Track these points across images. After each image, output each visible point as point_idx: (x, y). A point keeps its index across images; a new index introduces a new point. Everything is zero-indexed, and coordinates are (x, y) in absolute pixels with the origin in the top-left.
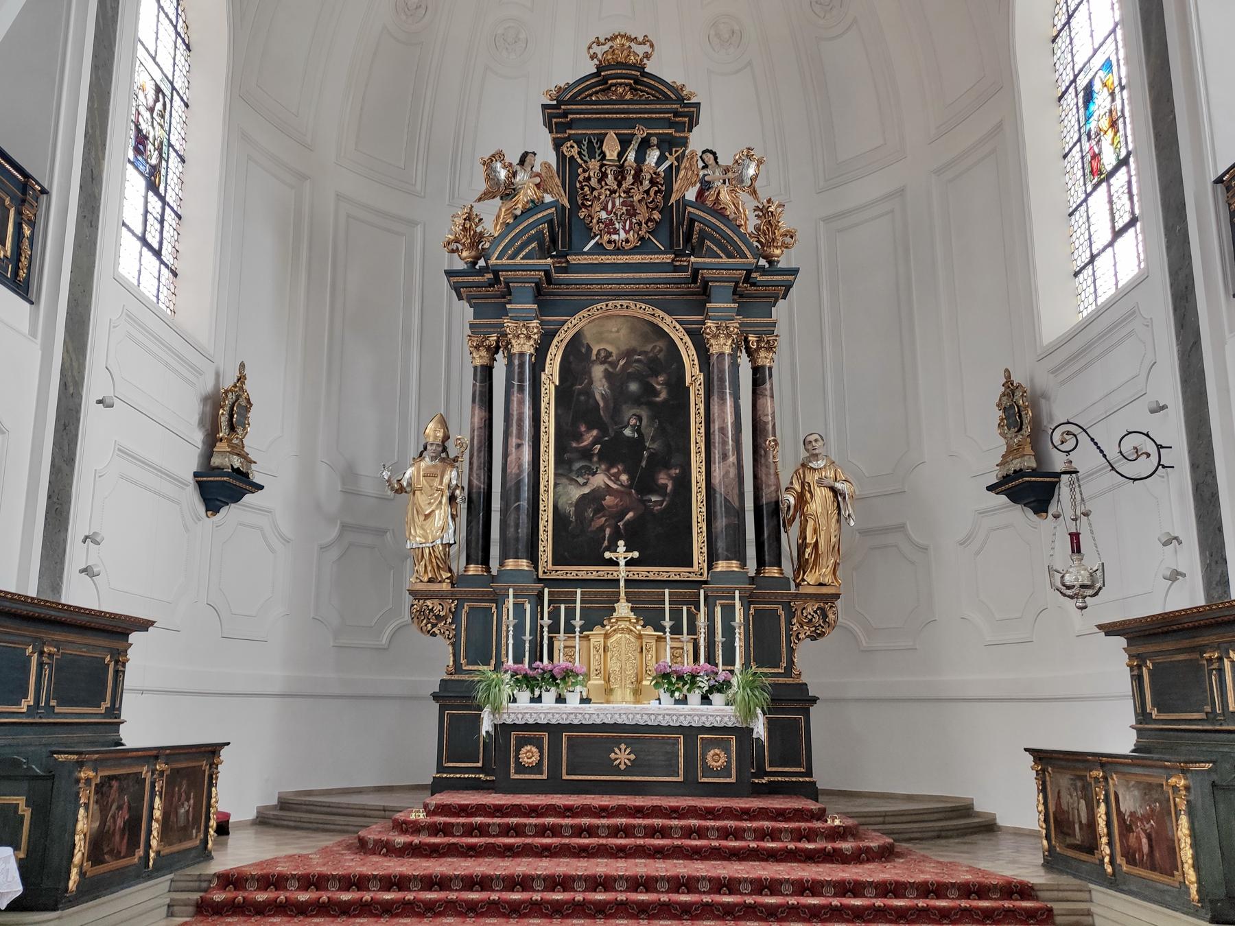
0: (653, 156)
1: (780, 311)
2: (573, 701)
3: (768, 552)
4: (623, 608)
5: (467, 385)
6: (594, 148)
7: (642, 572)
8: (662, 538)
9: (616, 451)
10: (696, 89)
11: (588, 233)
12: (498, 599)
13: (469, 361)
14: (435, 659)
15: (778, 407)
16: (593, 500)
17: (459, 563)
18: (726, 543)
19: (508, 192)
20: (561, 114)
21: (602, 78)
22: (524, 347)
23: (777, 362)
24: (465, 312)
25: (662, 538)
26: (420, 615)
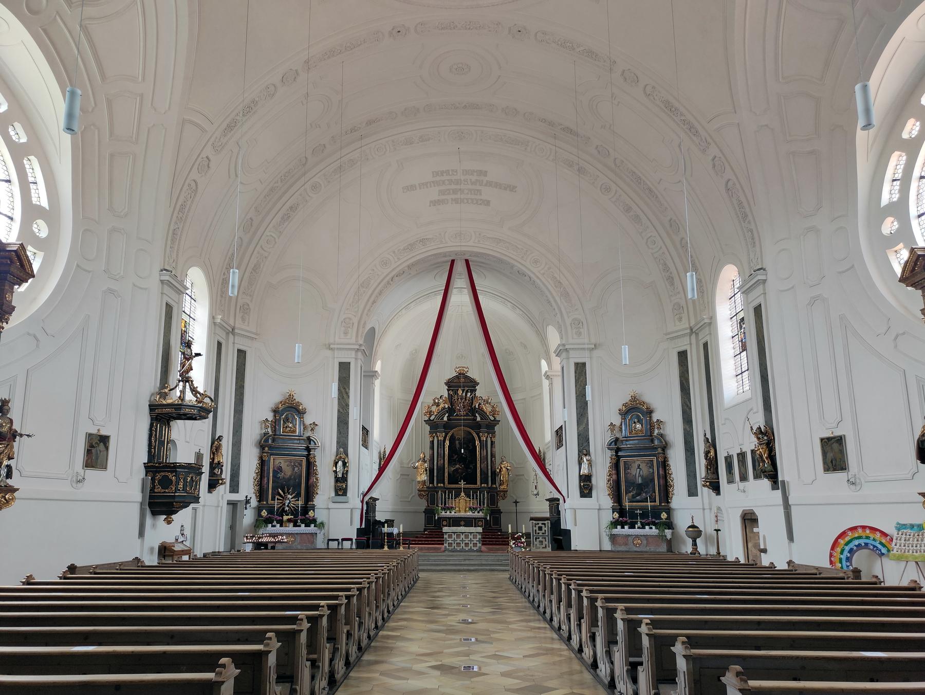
0: (469, 394)
1: (496, 428)
2: (453, 513)
3: (494, 482)
4: (463, 494)
5: (428, 445)
6: (456, 392)
7: (468, 486)
8: (471, 479)
9: (461, 459)
10: (478, 380)
11: (455, 412)
12: (437, 493)
13: (428, 439)
14: (423, 504)
15: (497, 450)
16: (457, 469)
17: (428, 484)
18: (484, 480)
19: (438, 405)
20: (450, 384)
21: (457, 377)
22: (441, 438)
23: (497, 440)
24: (428, 428)
25: (471, 479)
26: (420, 495)
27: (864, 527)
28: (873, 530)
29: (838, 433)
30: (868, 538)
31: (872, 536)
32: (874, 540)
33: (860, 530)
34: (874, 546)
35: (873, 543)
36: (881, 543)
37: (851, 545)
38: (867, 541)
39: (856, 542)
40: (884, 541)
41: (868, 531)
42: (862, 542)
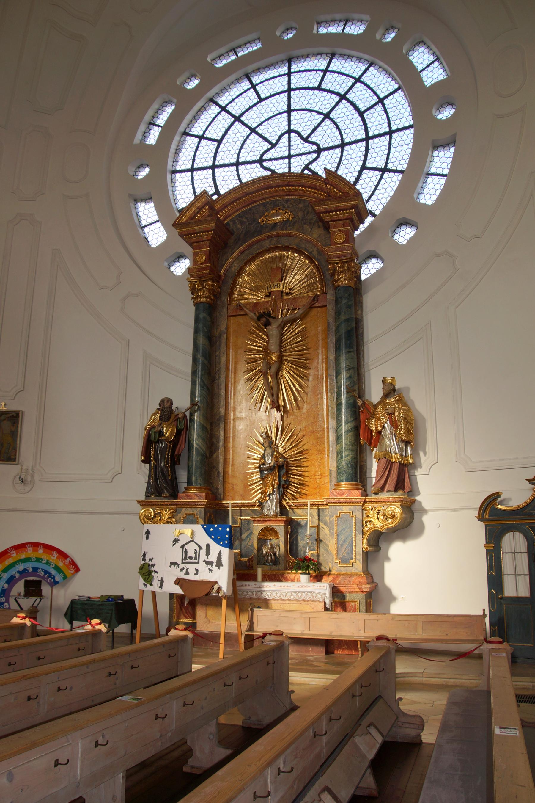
27: (36, 545)
28: (49, 548)
29: (13, 407)
30: (39, 560)
31: (45, 557)
32: (48, 563)
33: (30, 549)
34: (46, 572)
35: (46, 568)
36: (57, 568)
37: (13, 572)
38: (37, 565)
39: (21, 567)
40: (61, 564)
41: (41, 551)
42: (29, 566)
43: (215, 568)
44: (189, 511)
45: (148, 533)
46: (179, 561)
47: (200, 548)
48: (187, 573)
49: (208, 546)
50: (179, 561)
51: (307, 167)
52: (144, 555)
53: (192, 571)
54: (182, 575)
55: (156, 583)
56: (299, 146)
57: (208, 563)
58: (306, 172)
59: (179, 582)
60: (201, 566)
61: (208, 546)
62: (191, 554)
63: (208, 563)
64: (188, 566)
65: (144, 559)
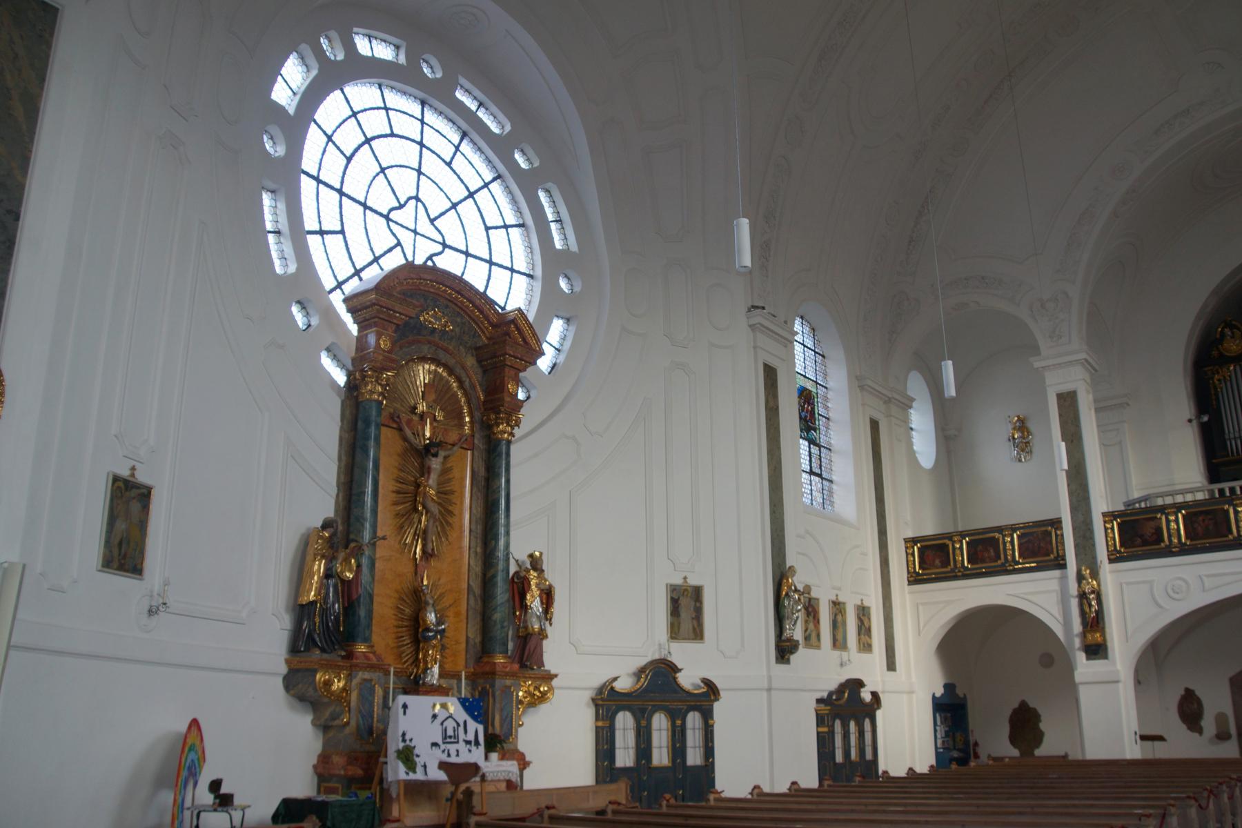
43: (473, 748)
44: (367, 675)
45: (405, 706)
46: (440, 741)
47: (458, 725)
48: (449, 755)
49: (465, 722)
50: (440, 741)
51: (430, 258)
52: (404, 734)
53: (453, 753)
54: (444, 758)
55: (419, 769)
56: (424, 226)
57: (468, 742)
58: (430, 263)
59: (443, 766)
60: (461, 746)
61: (465, 722)
62: (450, 732)
63: (468, 742)
64: (449, 746)
65: (404, 741)
